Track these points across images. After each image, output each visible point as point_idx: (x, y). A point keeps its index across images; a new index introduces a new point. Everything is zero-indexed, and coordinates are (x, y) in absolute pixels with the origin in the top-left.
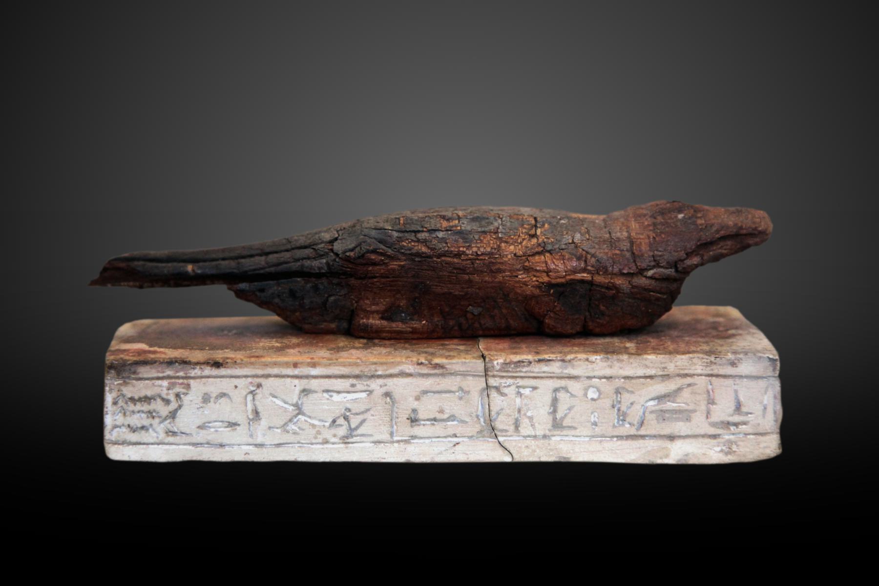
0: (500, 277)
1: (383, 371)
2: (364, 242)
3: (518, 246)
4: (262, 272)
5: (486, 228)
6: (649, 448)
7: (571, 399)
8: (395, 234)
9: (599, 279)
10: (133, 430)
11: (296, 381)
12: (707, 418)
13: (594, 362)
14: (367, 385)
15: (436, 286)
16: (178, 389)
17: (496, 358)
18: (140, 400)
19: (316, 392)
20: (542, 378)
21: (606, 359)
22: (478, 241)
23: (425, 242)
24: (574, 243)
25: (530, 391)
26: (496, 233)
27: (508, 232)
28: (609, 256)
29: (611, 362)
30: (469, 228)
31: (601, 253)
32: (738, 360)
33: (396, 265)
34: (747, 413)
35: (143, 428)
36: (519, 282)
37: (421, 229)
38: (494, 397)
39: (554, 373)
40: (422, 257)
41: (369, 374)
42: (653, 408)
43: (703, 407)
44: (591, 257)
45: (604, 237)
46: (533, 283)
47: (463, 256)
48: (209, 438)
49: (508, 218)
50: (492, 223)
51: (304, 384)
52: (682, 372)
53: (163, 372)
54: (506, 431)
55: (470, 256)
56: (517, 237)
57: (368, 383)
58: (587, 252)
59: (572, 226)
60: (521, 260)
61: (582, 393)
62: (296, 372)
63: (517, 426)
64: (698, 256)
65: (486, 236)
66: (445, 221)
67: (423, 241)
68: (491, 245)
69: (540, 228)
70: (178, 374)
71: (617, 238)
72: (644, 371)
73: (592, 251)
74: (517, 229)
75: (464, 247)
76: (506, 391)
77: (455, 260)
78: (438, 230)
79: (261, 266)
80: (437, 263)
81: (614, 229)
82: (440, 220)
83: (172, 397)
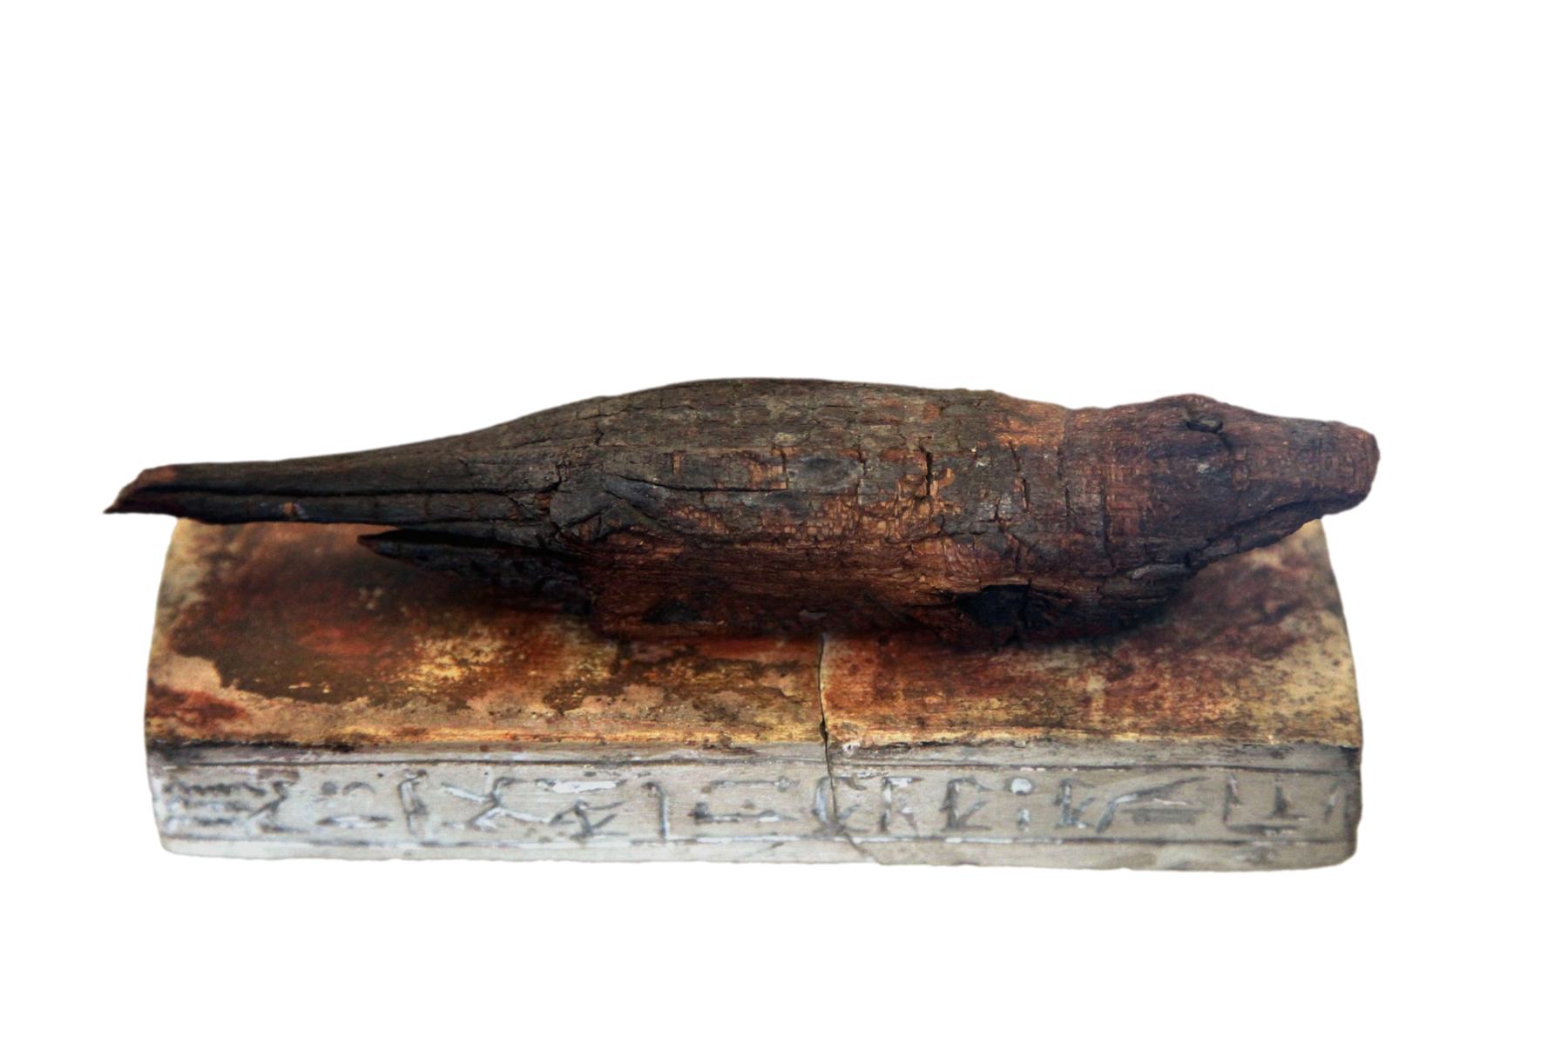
0: (859, 574)
1: (642, 756)
2: (607, 508)
3: (894, 521)
4: (421, 528)
5: (835, 485)
6: (1119, 854)
7: (982, 793)
8: (665, 494)
9: (1039, 582)
10: (206, 823)
11: (488, 768)
12: (1225, 819)
13: (1023, 748)
14: (615, 774)
15: (742, 584)
16: (276, 778)
17: (847, 736)
18: (211, 789)
19: (526, 781)
20: (928, 767)
21: (1046, 742)
22: (819, 515)
23: (717, 513)
24: (1000, 520)
25: (909, 782)
26: (853, 493)
27: (876, 494)
28: (1063, 546)
29: (1055, 747)
30: (802, 486)
31: (1047, 541)
32: (1286, 750)
33: (665, 553)
34: (1296, 817)
35: (220, 821)
36: (894, 583)
37: (712, 486)
38: (843, 791)
39: (950, 761)
40: (713, 542)
41: (617, 761)
42: (1128, 807)
43: (1218, 807)
44: (1028, 552)
45: (1056, 504)
46: (921, 587)
47: (790, 541)
48: (339, 835)
49: (878, 459)
50: (847, 474)
51: (501, 770)
52: (1182, 762)
53: (248, 757)
54: (865, 831)
55: (803, 543)
56: (892, 504)
57: (617, 771)
58: (1022, 542)
59: (997, 475)
60: (898, 550)
61: (999, 786)
62: (487, 756)
63: (883, 825)
64: (1231, 540)
65: (834, 503)
66: (758, 467)
67: (716, 511)
68: (844, 523)
69: (936, 478)
70: (274, 760)
71: (1080, 508)
72: (1115, 760)
73: (1031, 539)
74: (894, 487)
75: (791, 526)
76: (864, 783)
77: (776, 548)
78: (747, 490)
79: (416, 518)
80: (742, 551)
81: (1077, 483)
82: (749, 464)
83: (266, 785)
